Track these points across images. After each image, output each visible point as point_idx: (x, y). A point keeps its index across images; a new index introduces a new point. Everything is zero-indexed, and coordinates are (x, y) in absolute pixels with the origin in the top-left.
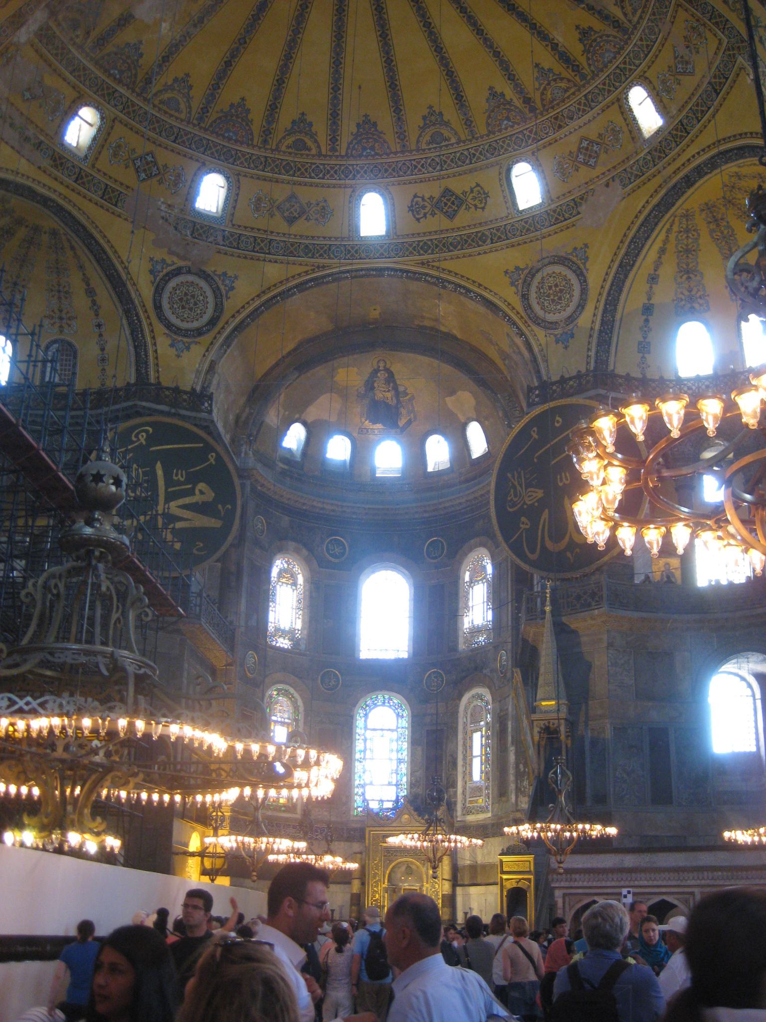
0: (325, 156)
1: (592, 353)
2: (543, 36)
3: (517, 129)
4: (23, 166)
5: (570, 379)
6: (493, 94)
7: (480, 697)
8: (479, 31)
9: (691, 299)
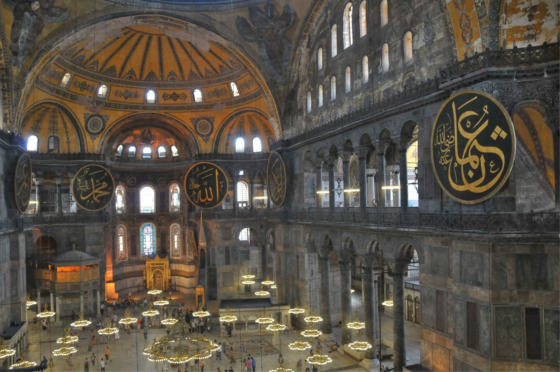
0: (138, 80)
1: (214, 146)
2: (208, 63)
3: (197, 81)
4: (48, 96)
5: (208, 154)
6: (191, 71)
7: (176, 226)
8: (190, 57)
9: (241, 133)
